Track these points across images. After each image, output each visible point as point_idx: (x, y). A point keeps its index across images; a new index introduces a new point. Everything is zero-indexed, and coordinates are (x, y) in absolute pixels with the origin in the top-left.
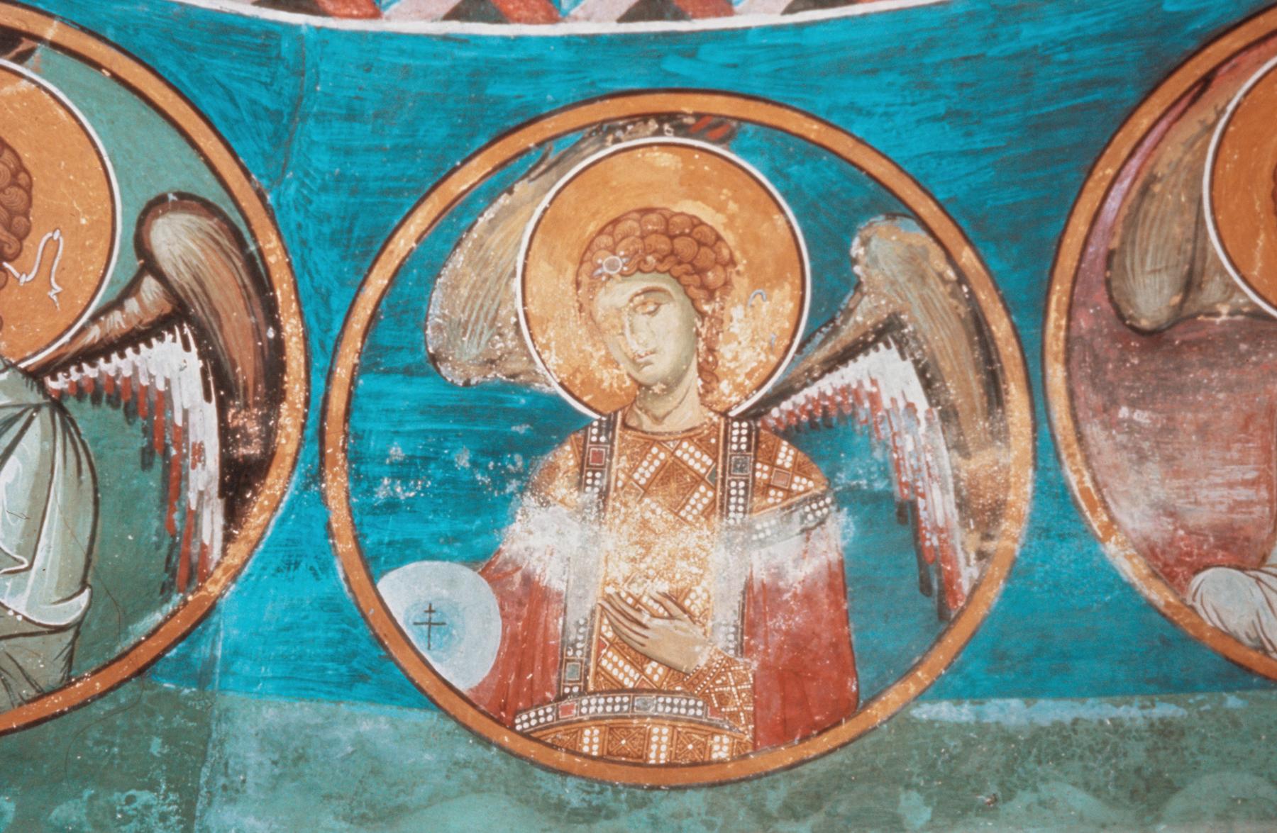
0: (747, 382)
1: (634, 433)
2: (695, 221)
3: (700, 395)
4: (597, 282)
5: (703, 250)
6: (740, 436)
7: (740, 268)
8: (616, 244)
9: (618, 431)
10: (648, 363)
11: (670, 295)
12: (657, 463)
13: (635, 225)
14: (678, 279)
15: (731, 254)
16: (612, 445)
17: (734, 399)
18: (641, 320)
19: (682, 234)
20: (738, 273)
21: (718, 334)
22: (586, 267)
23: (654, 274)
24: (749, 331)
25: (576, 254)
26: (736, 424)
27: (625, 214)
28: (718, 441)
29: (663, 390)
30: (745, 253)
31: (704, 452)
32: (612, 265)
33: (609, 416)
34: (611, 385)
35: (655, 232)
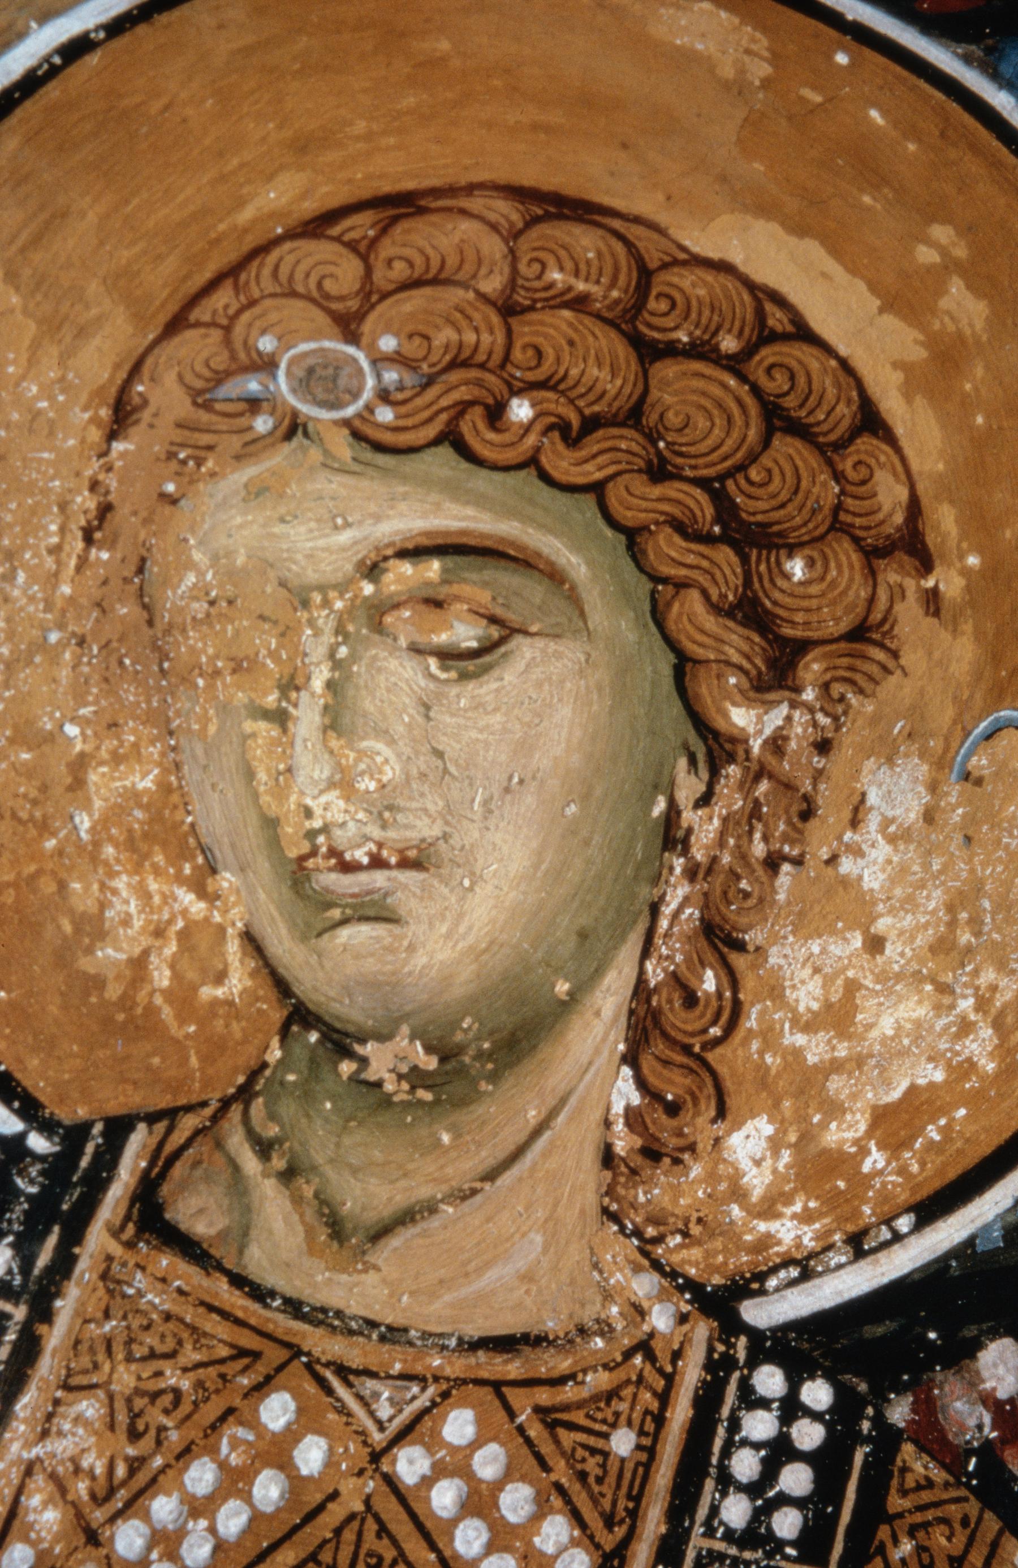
0: (875, 1159)
1: (186, 1274)
2: (777, 319)
3: (608, 1158)
4: (221, 423)
5: (786, 448)
6: (779, 1452)
7: (947, 580)
8: (371, 295)
9: (97, 1238)
10: (378, 912)
11: (574, 598)
12: (269, 1489)
13: (493, 247)
14: (633, 537)
15: (914, 508)
16: (42, 1311)
17: (788, 1232)
18: (395, 678)
19: (702, 351)
20: (932, 601)
21: (773, 863)
22: (196, 348)
23: (526, 478)
24: (934, 899)
25: (163, 281)
26: (770, 1381)
27: (451, 191)
28: (648, 1452)
29: (416, 1077)
30: (980, 526)
31: (555, 1496)
32: (321, 380)
33: (74, 1137)
34: (139, 964)
35: (579, 303)
